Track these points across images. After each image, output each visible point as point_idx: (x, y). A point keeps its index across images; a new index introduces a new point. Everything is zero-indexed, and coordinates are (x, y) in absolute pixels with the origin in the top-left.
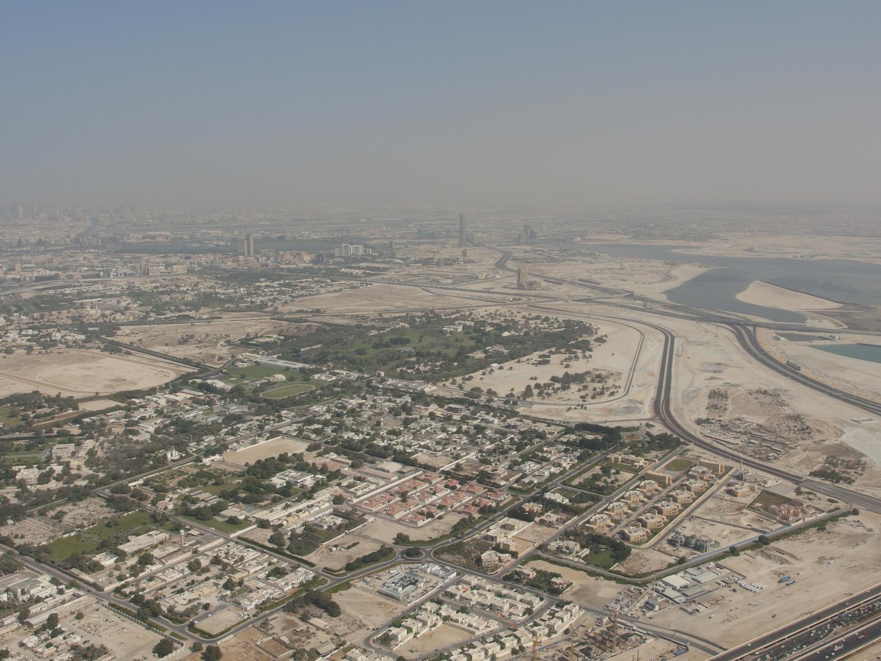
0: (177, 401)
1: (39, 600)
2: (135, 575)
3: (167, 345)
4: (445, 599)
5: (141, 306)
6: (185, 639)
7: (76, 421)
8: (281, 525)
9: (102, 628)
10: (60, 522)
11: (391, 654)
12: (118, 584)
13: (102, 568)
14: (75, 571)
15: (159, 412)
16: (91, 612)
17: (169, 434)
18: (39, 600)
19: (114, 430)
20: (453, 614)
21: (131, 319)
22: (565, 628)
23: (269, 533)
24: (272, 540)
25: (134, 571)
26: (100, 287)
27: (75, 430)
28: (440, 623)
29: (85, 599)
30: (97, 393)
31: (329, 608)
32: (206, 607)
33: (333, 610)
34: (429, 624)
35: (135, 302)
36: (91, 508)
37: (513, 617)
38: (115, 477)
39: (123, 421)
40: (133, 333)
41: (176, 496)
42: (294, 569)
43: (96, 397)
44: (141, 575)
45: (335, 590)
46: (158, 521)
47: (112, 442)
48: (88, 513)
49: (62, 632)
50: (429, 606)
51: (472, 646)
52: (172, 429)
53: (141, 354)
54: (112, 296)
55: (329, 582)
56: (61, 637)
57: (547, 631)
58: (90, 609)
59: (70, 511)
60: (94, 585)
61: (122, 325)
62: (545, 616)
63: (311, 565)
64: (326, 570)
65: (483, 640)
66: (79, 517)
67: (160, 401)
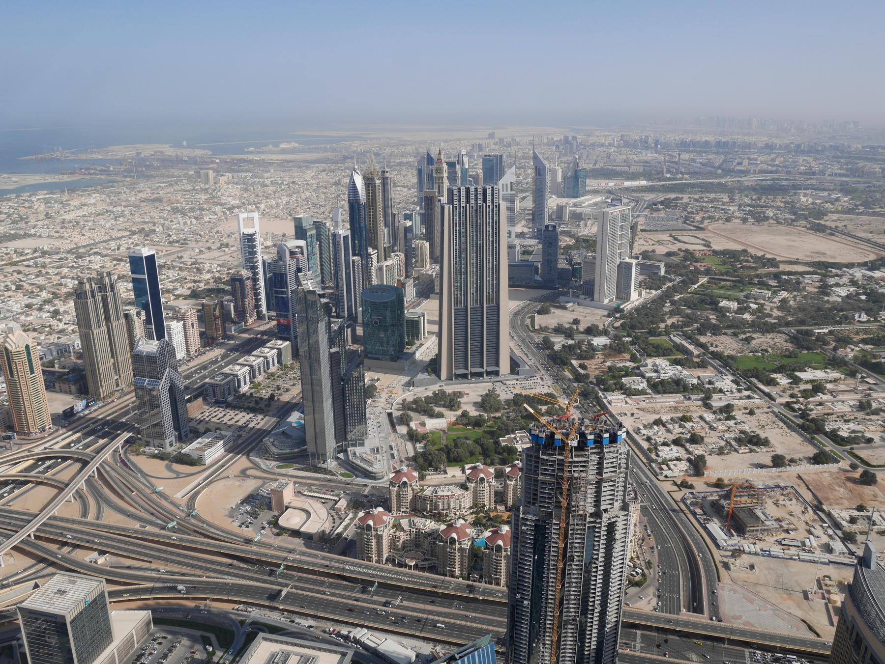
0: (872, 277)
1: (721, 391)
2: (806, 398)
3: (871, 232)
5: (851, 199)
6: (843, 459)
7: (776, 276)
9: (769, 427)
10: (749, 343)
12: (789, 400)
13: (778, 384)
14: (754, 380)
15: (853, 283)
16: (762, 413)
17: (861, 300)
18: (721, 391)
19: (807, 288)
21: (840, 208)
25: (806, 394)
26: (814, 182)
27: (773, 283)
29: (757, 401)
30: (797, 259)
32: (870, 441)
35: (846, 196)
36: (776, 340)
38: (802, 322)
39: (818, 284)
40: (839, 220)
41: (857, 349)
43: (796, 262)
44: (811, 399)
46: (835, 363)
47: (804, 297)
48: (773, 343)
49: (735, 419)
52: (863, 297)
53: (844, 237)
54: (824, 190)
56: (733, 422)
58: (761, 410)
59: (758, 338)
60: (768, 395)
61: (830, 212)
66: (765, 344)
67: (855, 274)
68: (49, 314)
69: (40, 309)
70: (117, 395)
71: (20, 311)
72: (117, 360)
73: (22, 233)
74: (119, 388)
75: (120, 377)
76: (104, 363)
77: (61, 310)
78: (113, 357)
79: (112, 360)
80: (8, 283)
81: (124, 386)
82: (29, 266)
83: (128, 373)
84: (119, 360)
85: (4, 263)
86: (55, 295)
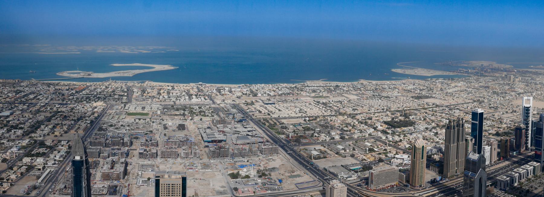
68: (433, 133)
69: (430, 131)
70: (455, 177)
71: (423, 130)
72: (458, 160)
73: (430, 95)
74: (456, 174)
75: (458, 169)
76: (453, 161)
77: (439, 133)
78: (457, 159)
79: (456, 160)
80: (421, 117)
81: (459, 173)
82: (430, 111)
83: (462, 167)
84: (459, 160)
85: (421, 108)
86: (438, 125)
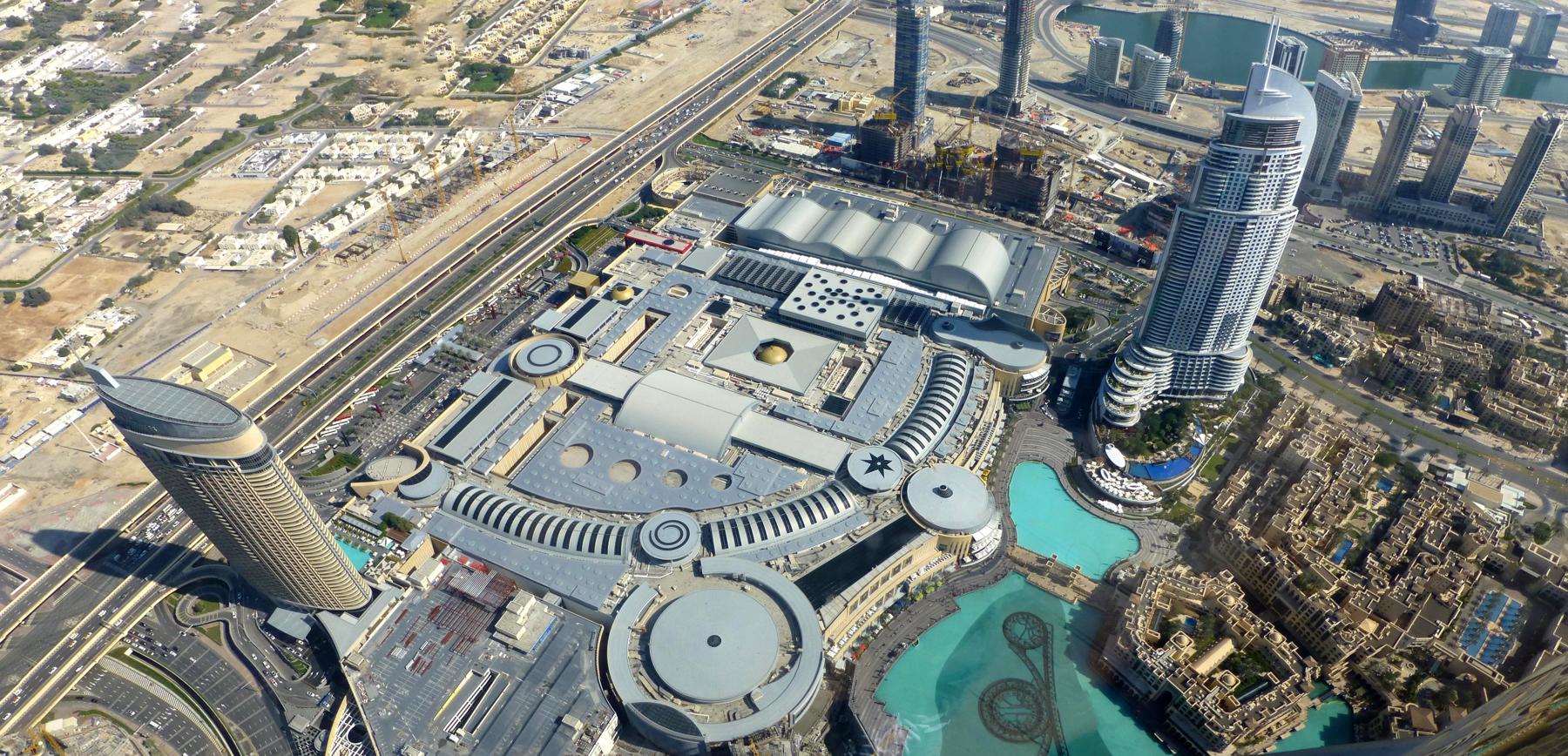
4: (321, 161)
8: (74, 145)
11: (275, 229)
20: (336, 173)
22: (463, 152)
23: (59, 158)
24: (65, 163)
28: (322, 184)
31: (177, 208)
33: (183, 210)
34: (310, 190)
37: (404, 158)
42: (112, 184)
45: (178, 190)
50: (303, 172)
51: (364, 195)
55: (167, 185)
57: (444, 158)
62: (439, 147)
63: (135, 174)
64: (157, 174)
65: (377, 185)
